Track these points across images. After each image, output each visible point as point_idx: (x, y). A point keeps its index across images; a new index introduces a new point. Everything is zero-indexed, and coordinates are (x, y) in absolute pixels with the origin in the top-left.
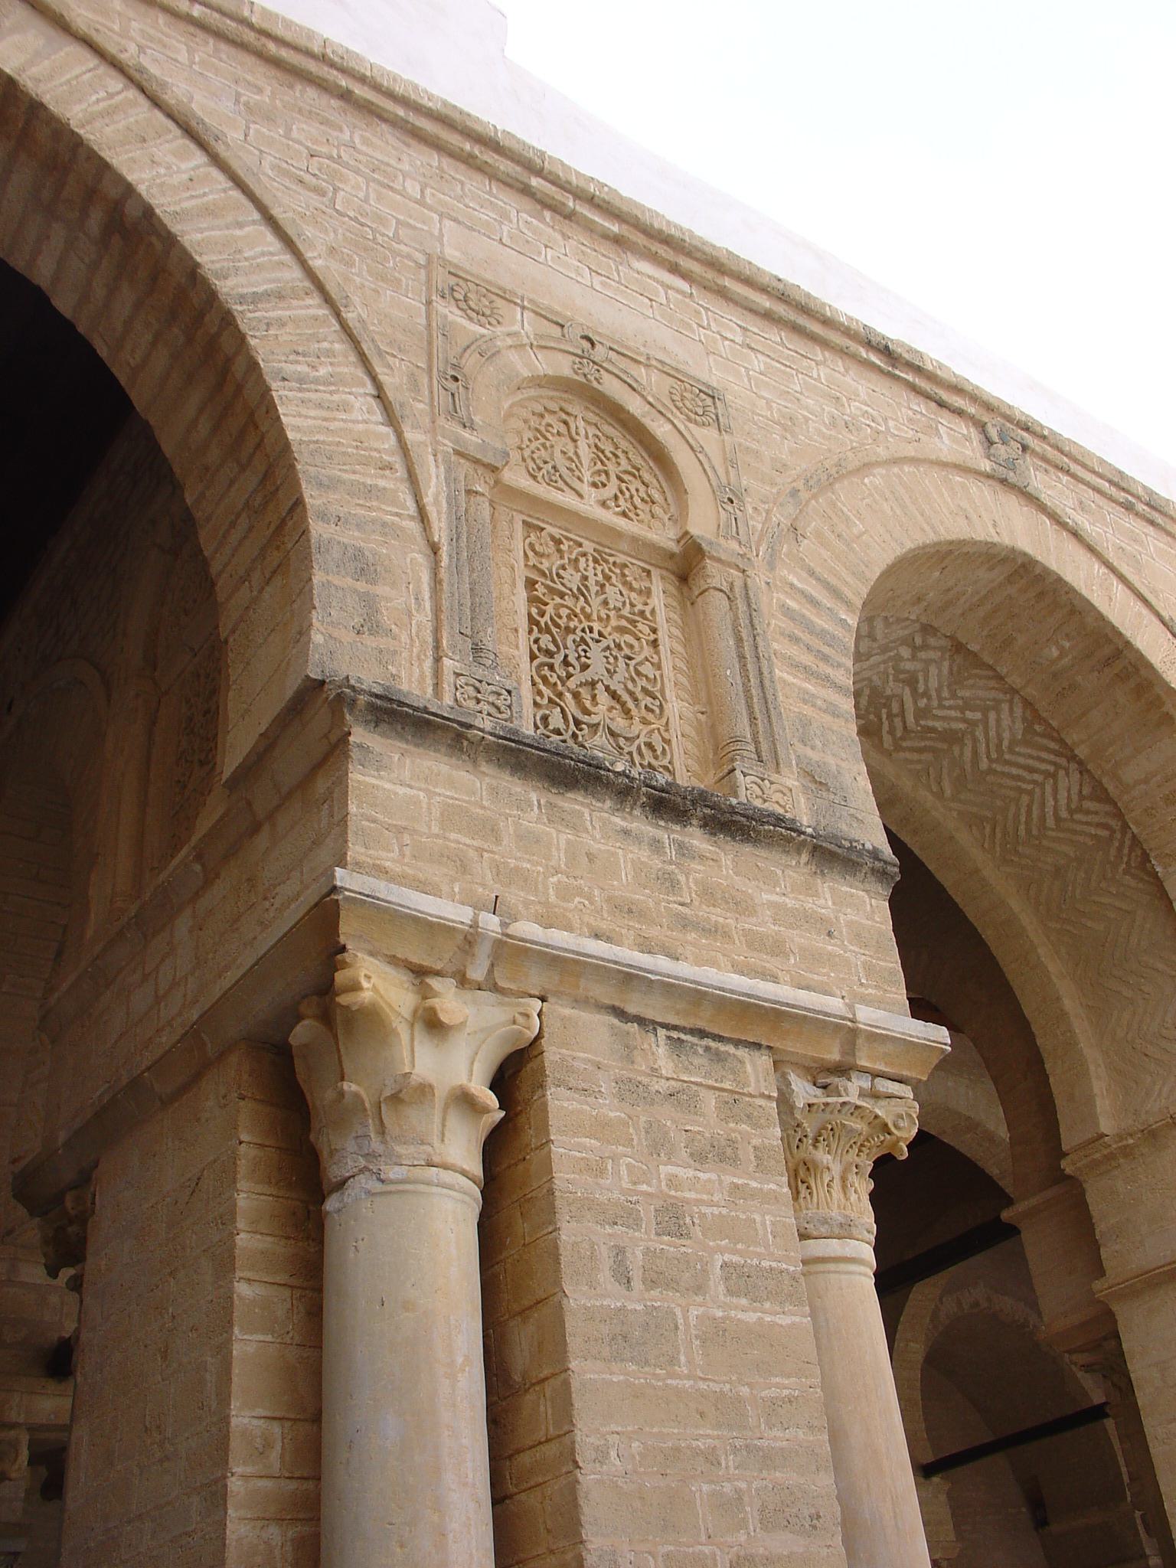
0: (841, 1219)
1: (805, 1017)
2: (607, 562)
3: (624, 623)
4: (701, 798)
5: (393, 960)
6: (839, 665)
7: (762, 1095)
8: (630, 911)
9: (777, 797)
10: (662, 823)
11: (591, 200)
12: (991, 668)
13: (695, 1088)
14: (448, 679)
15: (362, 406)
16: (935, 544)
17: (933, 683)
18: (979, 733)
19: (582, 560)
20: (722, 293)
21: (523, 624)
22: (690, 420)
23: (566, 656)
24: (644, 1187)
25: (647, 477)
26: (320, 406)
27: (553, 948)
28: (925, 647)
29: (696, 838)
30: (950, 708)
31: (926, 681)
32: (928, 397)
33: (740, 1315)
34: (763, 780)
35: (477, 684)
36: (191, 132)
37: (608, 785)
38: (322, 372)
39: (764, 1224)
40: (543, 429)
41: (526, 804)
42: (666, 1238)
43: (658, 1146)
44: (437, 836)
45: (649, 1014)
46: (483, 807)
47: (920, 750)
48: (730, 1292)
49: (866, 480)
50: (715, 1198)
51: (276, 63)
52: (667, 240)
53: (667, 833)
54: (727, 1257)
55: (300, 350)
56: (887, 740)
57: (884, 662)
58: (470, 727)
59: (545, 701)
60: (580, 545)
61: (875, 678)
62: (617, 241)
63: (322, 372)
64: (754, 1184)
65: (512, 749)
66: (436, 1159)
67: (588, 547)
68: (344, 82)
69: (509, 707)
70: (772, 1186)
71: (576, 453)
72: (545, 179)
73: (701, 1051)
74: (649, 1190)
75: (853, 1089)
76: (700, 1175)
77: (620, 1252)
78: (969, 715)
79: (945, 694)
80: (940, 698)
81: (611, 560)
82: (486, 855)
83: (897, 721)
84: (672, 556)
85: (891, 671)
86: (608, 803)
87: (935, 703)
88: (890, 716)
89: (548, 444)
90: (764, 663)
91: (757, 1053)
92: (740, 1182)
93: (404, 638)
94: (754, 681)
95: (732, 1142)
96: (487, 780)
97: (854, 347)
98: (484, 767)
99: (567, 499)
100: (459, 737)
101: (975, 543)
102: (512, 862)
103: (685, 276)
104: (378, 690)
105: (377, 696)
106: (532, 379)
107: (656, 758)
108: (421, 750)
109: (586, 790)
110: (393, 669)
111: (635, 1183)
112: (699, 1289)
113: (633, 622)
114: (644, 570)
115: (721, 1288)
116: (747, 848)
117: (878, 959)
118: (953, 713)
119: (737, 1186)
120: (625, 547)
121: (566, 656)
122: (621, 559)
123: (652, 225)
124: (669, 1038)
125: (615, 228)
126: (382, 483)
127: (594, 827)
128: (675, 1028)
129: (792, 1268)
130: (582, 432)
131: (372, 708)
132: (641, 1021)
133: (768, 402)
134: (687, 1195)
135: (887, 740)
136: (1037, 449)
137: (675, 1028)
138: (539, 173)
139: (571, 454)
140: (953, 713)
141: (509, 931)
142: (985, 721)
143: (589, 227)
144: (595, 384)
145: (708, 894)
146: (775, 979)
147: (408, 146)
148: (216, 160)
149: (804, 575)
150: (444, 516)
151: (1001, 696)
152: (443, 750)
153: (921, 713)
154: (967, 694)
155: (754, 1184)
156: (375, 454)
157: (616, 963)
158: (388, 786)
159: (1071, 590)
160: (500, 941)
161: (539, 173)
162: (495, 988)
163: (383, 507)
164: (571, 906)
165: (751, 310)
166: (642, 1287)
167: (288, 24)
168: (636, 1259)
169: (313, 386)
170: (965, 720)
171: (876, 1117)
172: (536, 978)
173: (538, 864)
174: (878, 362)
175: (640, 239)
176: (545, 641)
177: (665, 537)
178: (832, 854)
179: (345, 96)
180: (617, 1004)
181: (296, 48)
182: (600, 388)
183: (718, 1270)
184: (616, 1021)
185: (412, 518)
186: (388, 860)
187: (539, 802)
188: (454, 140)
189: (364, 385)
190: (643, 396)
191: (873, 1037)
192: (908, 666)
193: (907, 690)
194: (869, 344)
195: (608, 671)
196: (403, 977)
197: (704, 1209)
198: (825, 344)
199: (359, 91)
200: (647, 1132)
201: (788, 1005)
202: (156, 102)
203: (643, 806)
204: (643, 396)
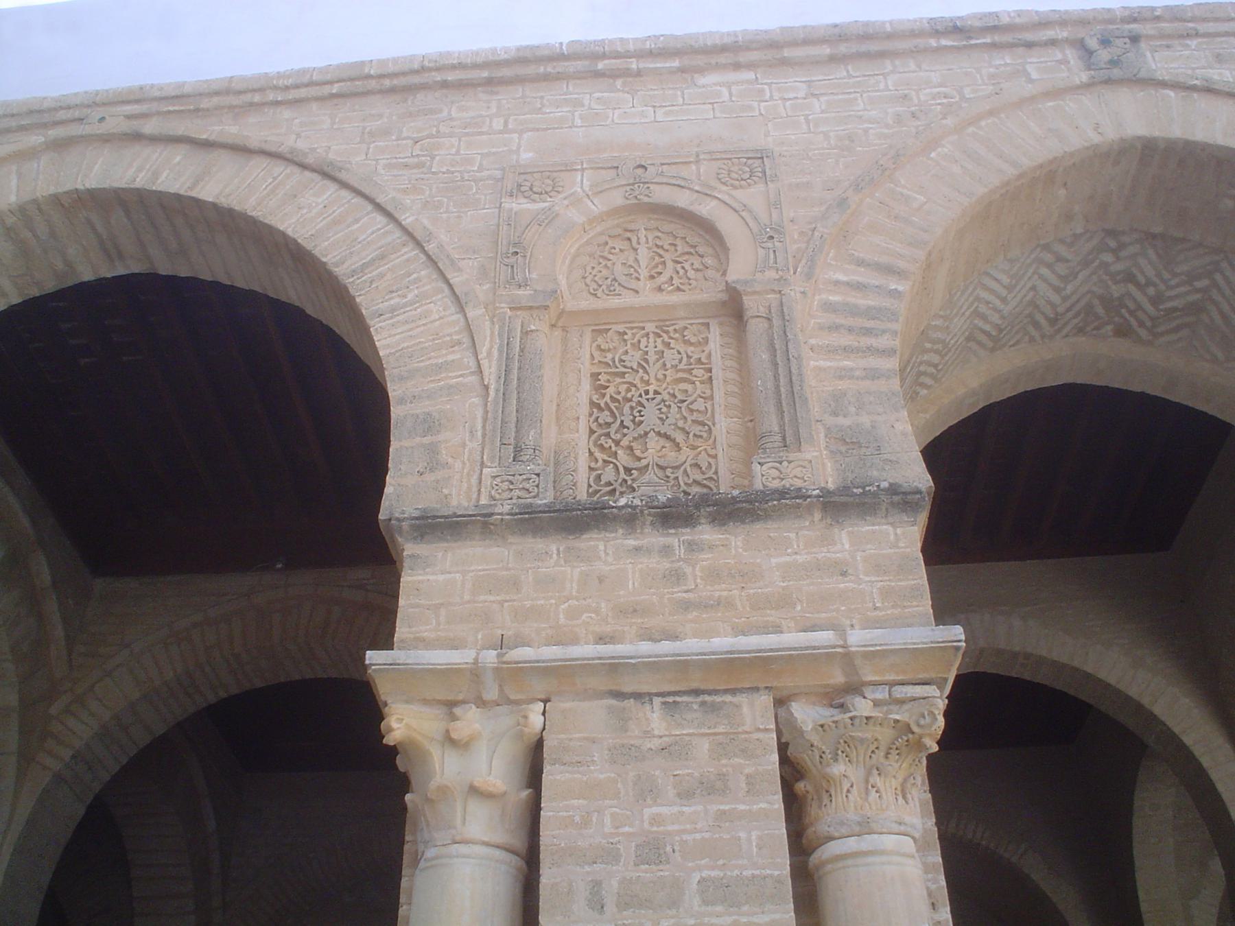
0: (857, 818)
1: (791, 655)
2: (667, 332)
3: (680, 375)
4: (704, 501)
5: (426, 702)
6: (884, 332)
7: (759, 730)
8: (635, 611)
9: (798, 472)
10: (672, 531)
11: (651, 54)
12: (1183, 240)
13: (687, 738)
14: (487, 481)
15: (439, 309)
16: (1020, 176)
17: (1150, 272)
18: (1215, 294)
19: (644, 341)
20: (784, 62)
21: (585, 409)
22: (735, 188)
24: (627, 829)
25: (701, 250)
27: (543, 662)
28: (1122, 246)
29: (706, 533)
30: (1177, 286)
31: (1142, 272)
32: (1012, 46)
33: (714, 920)
34: (781, 463)
35: (511, 478)
36: (327, 173)
37: (615, 518)
38: (410, 296)
39: (749, 840)
40: (606, 254)
41: (550, 555)
42: (643, 867)
43: (647, 791)
44: (469, 602)
45: (645, 688)
46: (510, 569)
47: (1177, 329)
48: (705, 902)
49: (933, 155)
50: (699, 826)
51: (392, 90)
52: (723, 49)
53: (677, 539)
54: (705, 874)
55: (394, 288)
56: (1143, 333)
57: (1094, 273)
59: (600, 463)
60: (643, 328)
61: (1095, 289)
62: (682, 70)
63: (410, 296)
64: (742, 807)
65: (526, 520)
66: (458, 838)
67: (650, 327)
68: (438, 77)
69: (537, 486)
70: (763, 805)
71: (636, 260)
72: (610, 58)
73: (695, 707)
74: (631, 830)
75: (862, 706)
76: (685, 809)
77: (597, 884)
78: (1198, 284)
79: (1166, 276)
80: (1164, 282)
81: (671, 329)
82: (506, 604)
83: (1139, 313)
84: (724, 303)
85: (1105, 277)
86: (621, 531)
87: (1162, 287)
88: (1131, 313)
89: (609, 264)
90: (794, 362)
91: (756, 695)
92: (727, 807)
93: (458, 465)
94: (783, 381)
95: (722, 776)
96: (514, 547)
97: (921, 42)
98: (511, 539)
99: (627, 299)
100: (485, 525)
101: (1072, 154)
102: (528, 604)
103: (751, 66)
104: (416, 514)
105: (417, 518)
106: (591, 221)
107: (703, 473)
108: (459, 543)
109: (598, 528)
110: (446, 491)
111: (617, 828)
112: (674, 903)
113: (690, 371)
114: (703, 324)
115: (696, 901)
116: (758, 526)
117: (900, 580)
118: (1183, 289)
119: (724, 812)
120: (682, 314)
122: (682, 324)
123: (706, 45)
124: (664, 703)
125: (676, 63)
126: (450, 357)
127: (607, 554)
128: (670, 694)
129: (776, 873)
130: (643, 240)
131: (415, 528)
132: (638, 696)
133: (826, 135)
134: (669, 828)
135: (1143, 333)
136: (1151, 32)
137: (670, 694)
138: (604, 56)
139: (631, 262)
140: (1183, 289)
141: (505, 659)
142: (1215, 284)
143: (656, 72)
144: (646, 200)
145: (714, 575)
146: (778, 630)
147: (497, 93)
148: (344, 185)
150: (494, 363)
151: (1217, 258)
152: (477, 537)
153: (1156, 301)
154: (1184, 268)
155: (742, 807)
157: (600, 658)
158: (431, 578)
159: (1204, 146)
160: (497, 668)
161: (604, 56)
162: (510, 702)
164: (579, 622)
165: (817, 62)
166: (615, 910)
167: (395, 61)
168: (612, 886)
170: (1198, 291)
171: (897, 721)
172: (539, 687)
173: (551, 598)
174: (950, 43)
175: (700, 60)
176: (605, 417)
177: (709, 292)
178: (845, 506)
179: (445, 85)
180: (614, 688)
181: (404, 74)
182: (650, 200)
183: (695, 886)
184: (613, 702)
185: (473, 373)
186: (426, 631)
187: (558, 550)
188: (531, 70)
189: (443, 291)
190: (689, 189)
191: (871, 656)
192: (1119, 267)
193: (1131, 288)
194: (937, 33)
195: (661, 419)
196: (439, 711)
197: (685, 837)
198: (894, 54)
199: (451, 77)
200: (635, 784)
201: (772, 650)
202: (304, 167)
203: (652, 524)
204: (689, 189)
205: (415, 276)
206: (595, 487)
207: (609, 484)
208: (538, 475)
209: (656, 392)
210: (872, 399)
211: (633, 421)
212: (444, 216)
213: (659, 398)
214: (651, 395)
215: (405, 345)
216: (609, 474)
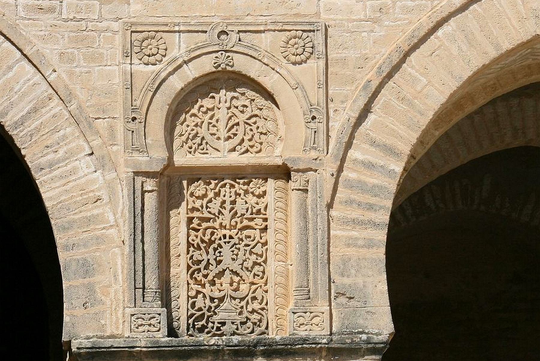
23: (209, 260)
26: (61, 177)
38: (61, 153)
58: (133, 347)
63: (61, 153)
110: (103, 322)
121: (209, 260)
126: (95, 212)
149: (367, 146)
156: (91, 194)
163: (97, 227)
169: (57, 166)
205: (62, 132)
206: (192, 311)
207: (200, 309)
208: (160, 314)
209: (231, 237)
210: (366, 264)
211: (215, 259)
212: (77, 70)
213: (232, 241)
214: (227, 239)
215: (63, 198)
216: (200, 303)
